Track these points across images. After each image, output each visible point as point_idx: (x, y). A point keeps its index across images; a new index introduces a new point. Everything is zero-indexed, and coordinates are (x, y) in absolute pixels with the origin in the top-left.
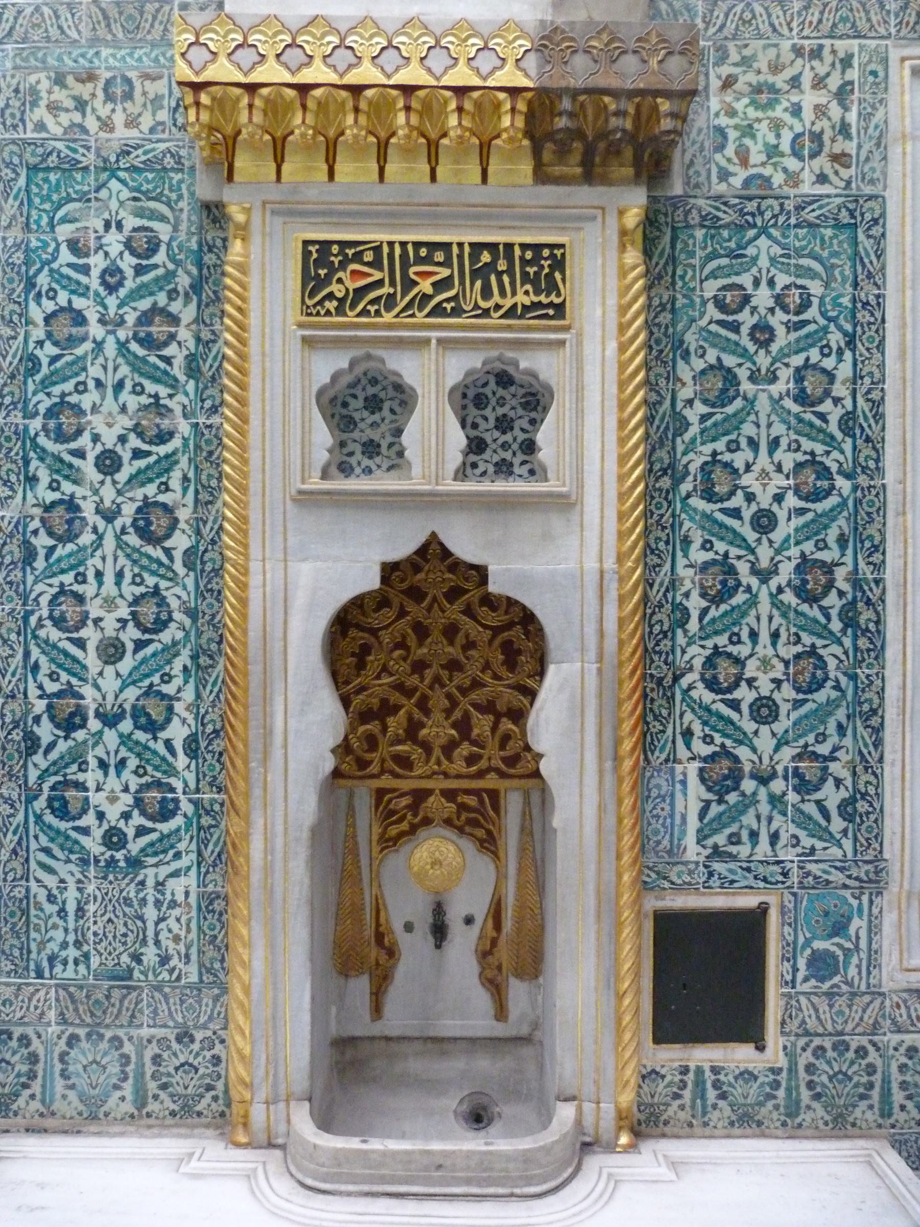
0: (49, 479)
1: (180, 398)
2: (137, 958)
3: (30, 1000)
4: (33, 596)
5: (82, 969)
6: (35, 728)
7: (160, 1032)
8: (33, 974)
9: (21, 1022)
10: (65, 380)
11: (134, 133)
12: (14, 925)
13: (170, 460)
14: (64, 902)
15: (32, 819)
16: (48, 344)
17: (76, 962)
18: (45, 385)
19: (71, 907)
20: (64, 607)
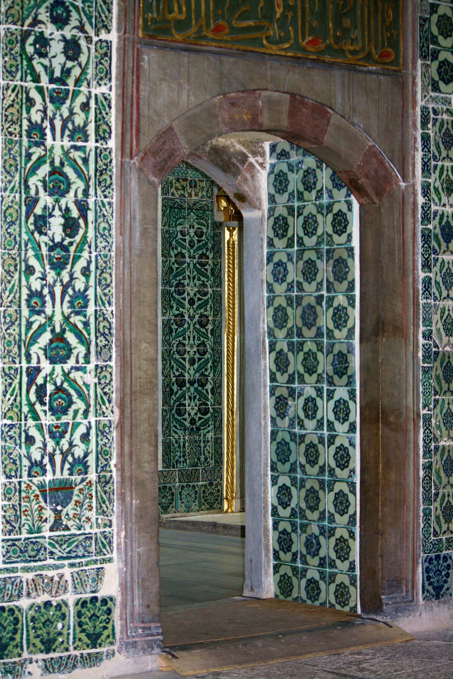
1: (210, 282)
2: (199, 459)
7: (204, 483)
9: (169, 483)
11: (197, 198)
13: (207, 301)
18: (176, 276)
19: (182, 444)
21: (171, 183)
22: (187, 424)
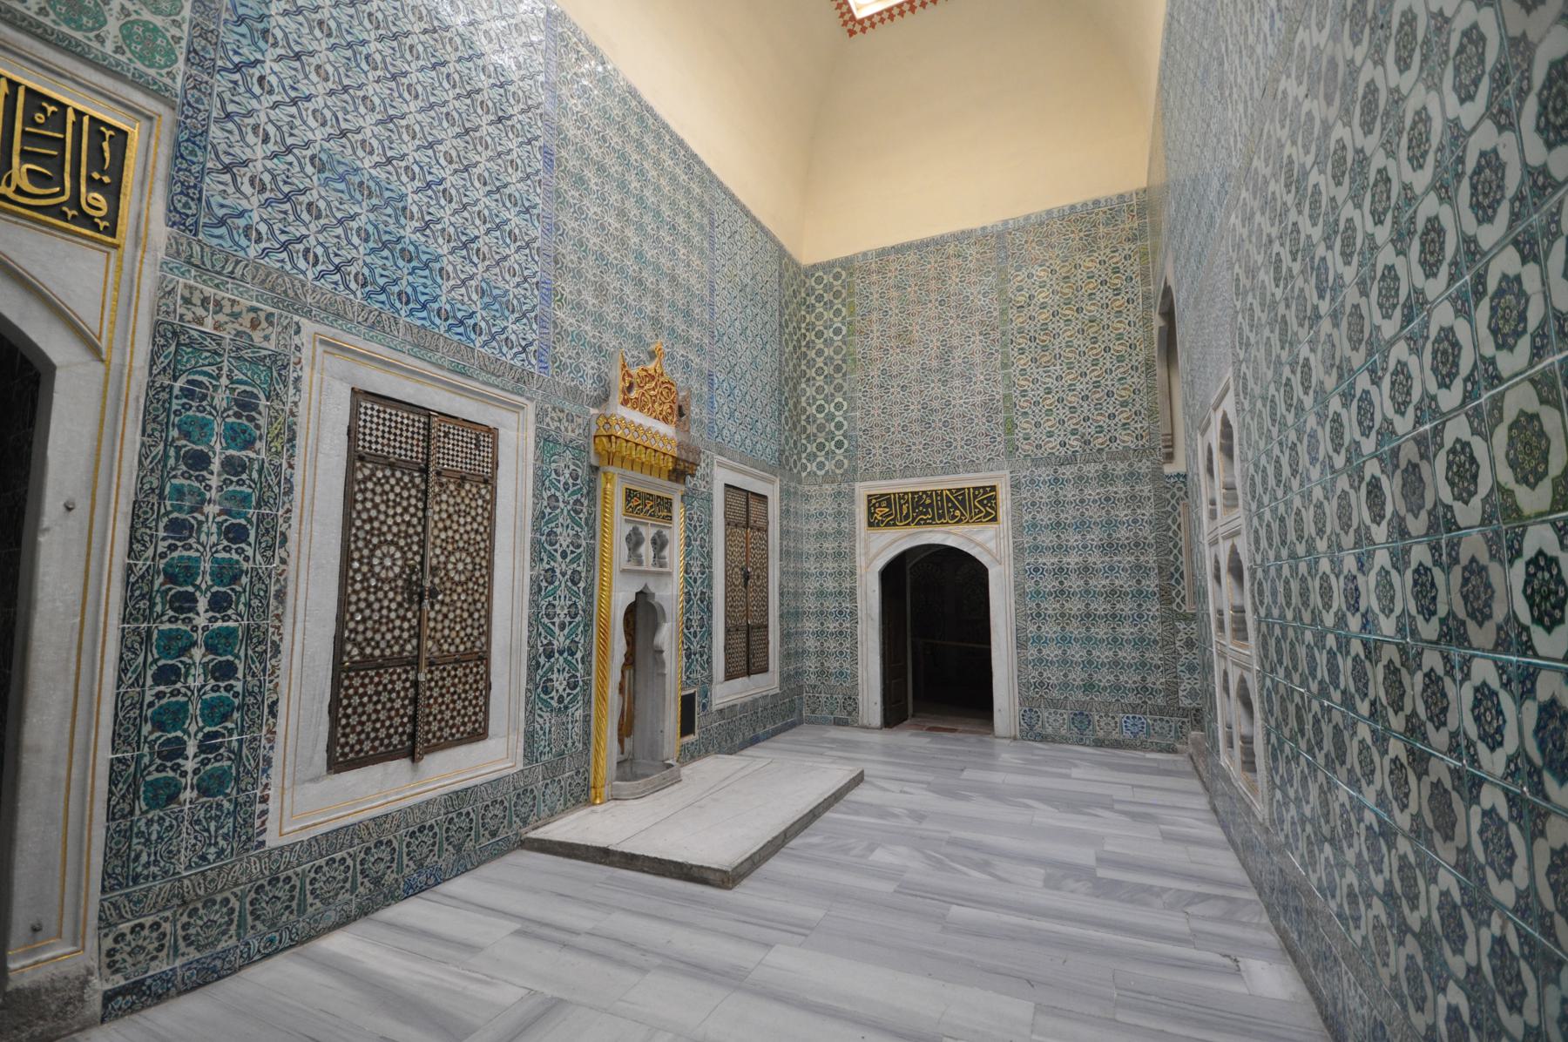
22: (554, 703)
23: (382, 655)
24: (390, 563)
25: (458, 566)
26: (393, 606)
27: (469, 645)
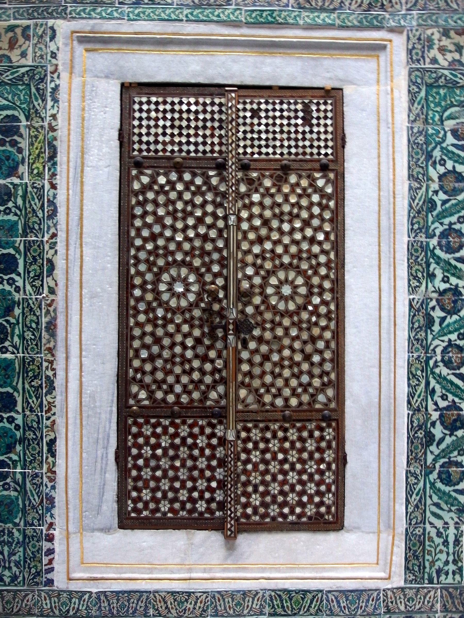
0: (442, 276)
3: (425, 597)
4: (432, 347)
5: (457, 577)
6: (432, 429)
8: (426, 581)
10: (452, 215)
12: (415, 551)
14: (447, 536)
15: (428, 486)
16: (441, 193)
17: (454, 573)
18: (439, 218)
19: (451, 539)
20: (451, 354)
21: (430, 40)
23: (178, 402)
24: (182, 289)
25: (284, 289)
26: (190, 342)
27: (305, 398)
